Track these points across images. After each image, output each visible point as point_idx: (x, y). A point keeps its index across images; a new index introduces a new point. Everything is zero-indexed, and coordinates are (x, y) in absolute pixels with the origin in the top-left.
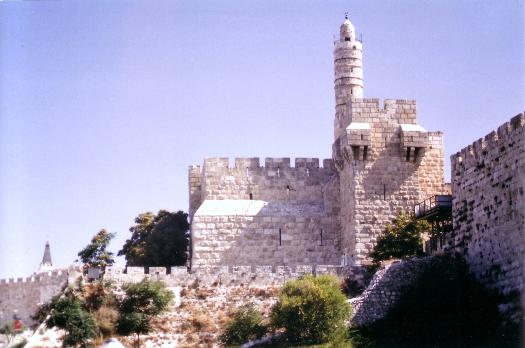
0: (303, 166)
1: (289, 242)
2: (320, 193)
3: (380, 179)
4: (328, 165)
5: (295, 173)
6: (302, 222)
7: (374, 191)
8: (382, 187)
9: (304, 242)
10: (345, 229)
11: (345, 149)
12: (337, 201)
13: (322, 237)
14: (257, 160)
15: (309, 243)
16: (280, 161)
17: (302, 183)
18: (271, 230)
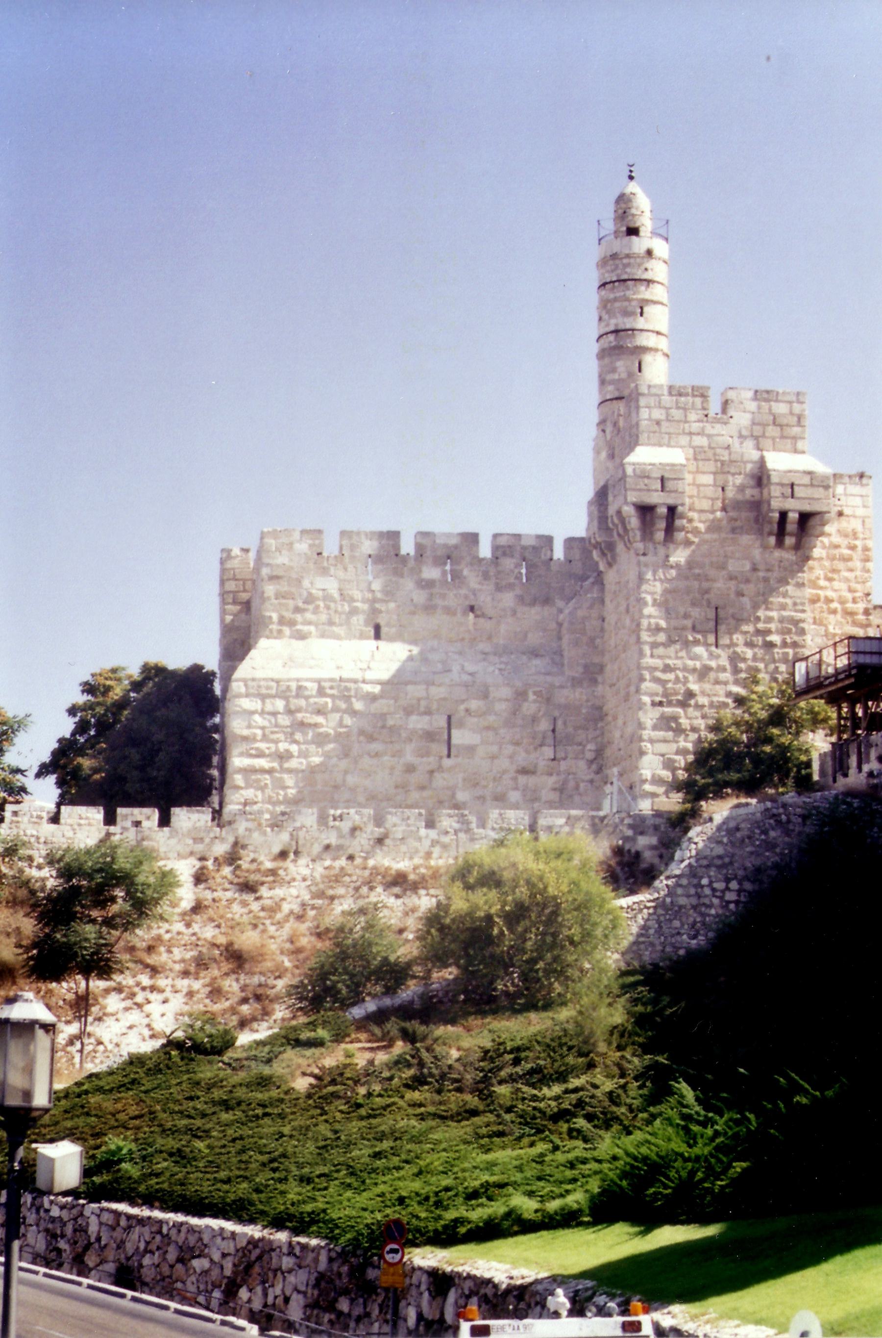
0: (512, 556)
1: (471, 750)
2: (554, 625)
3: (707, 591)
4: (577, 554)
5: (492, 574)
6: (507, 700)
7: (688, 623)
8: (711, 614)
9: (509, 749)
10: (615, 718)
11: (619, 512)
12: (596, 648)
13: (555, 737)
14: (394, 536)
15: (523, 754)
16: (454, 541)
17: (508, 599)
18: (427, 718)
